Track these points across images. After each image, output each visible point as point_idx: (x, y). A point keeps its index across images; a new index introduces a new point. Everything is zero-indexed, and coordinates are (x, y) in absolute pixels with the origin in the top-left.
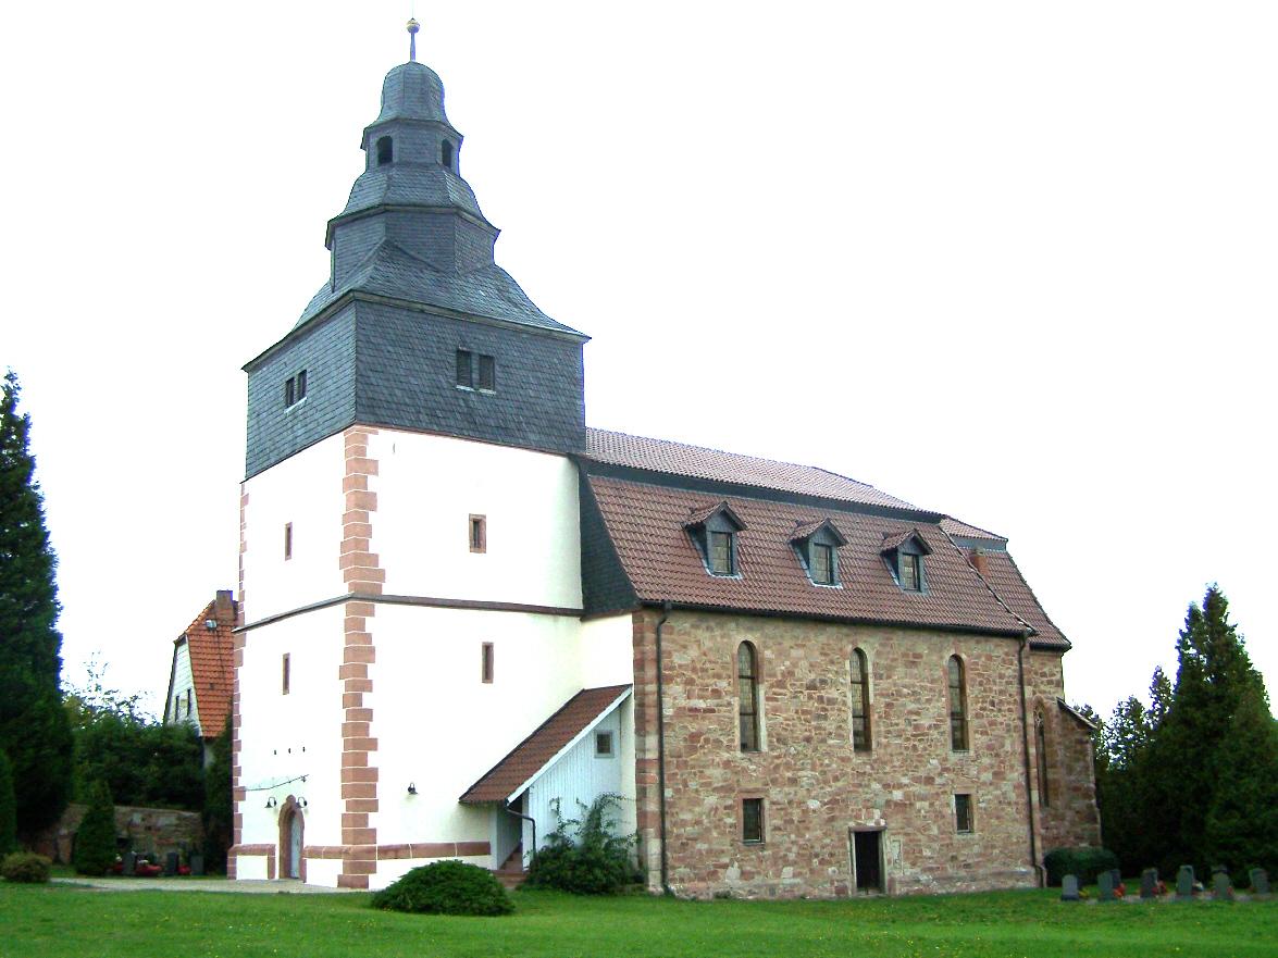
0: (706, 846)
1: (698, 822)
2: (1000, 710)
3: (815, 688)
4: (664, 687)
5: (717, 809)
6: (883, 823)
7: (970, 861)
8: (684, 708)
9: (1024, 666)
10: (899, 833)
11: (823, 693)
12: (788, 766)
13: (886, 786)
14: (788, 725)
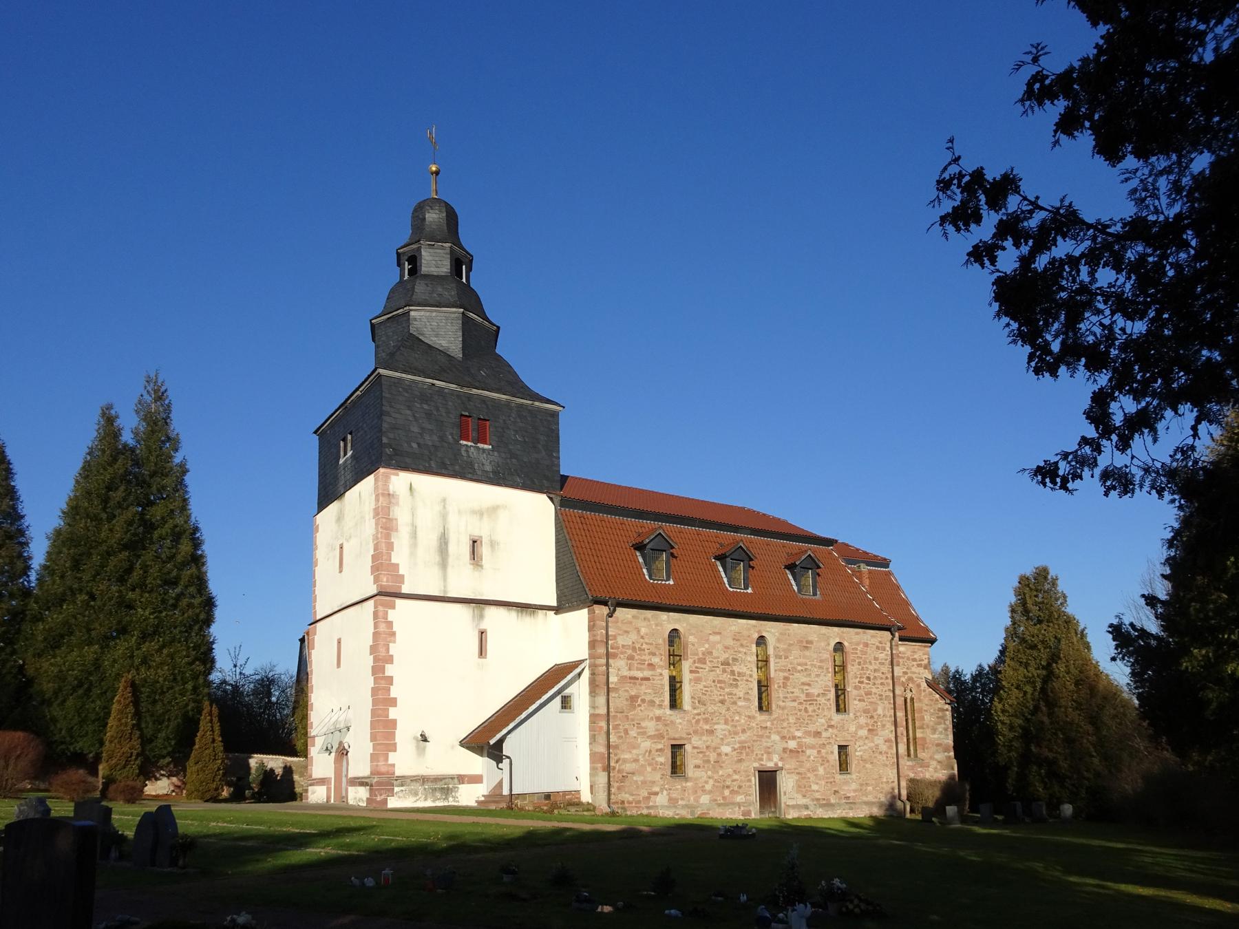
0: (642, 778)
1: (636, 761)
3: (728, 664)
4: (611, 661)
5: (650, 751)
6: (780, 764)
7: (848, 795)
8: (626, 677)
9: (894, 652)
10: (793, 773)
11: (735, 668)
12: (706, 721)
13: (783, 738)
14: (707, 691)
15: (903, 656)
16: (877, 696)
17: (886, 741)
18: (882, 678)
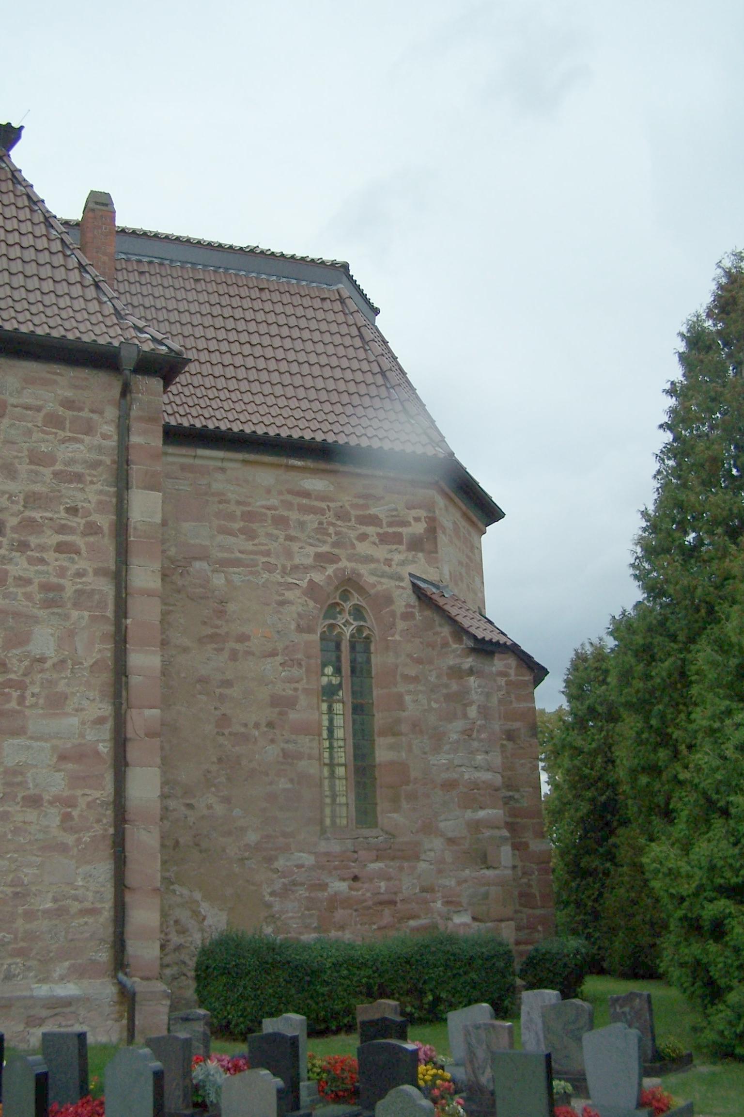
2: (23, 546)
9: (135, 439)
15: (323, 505)
16: (33, 588)
17: (63, 758)
18: (63, 529)
